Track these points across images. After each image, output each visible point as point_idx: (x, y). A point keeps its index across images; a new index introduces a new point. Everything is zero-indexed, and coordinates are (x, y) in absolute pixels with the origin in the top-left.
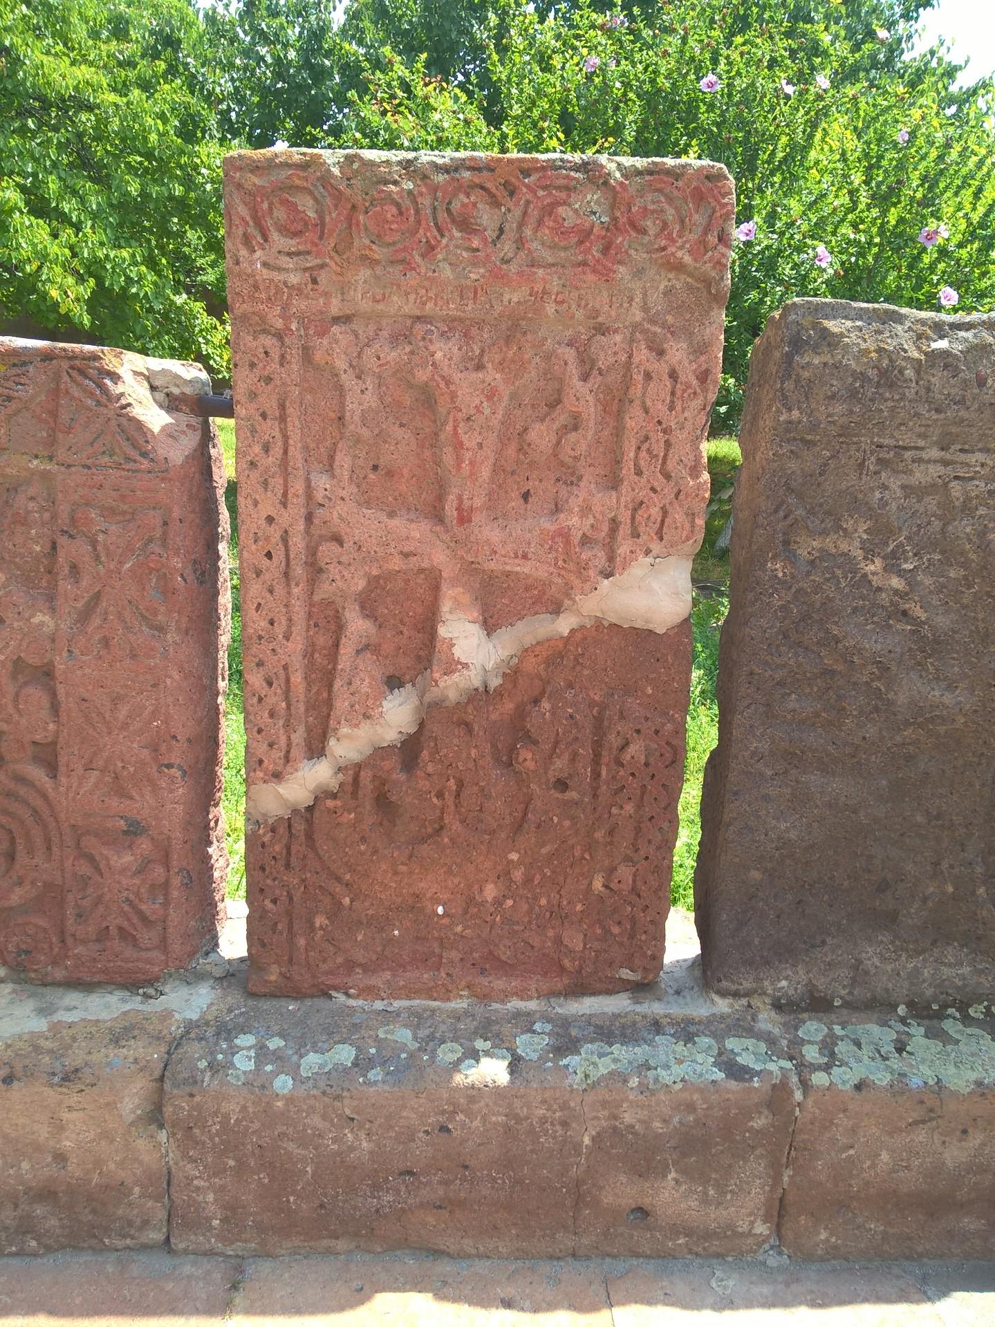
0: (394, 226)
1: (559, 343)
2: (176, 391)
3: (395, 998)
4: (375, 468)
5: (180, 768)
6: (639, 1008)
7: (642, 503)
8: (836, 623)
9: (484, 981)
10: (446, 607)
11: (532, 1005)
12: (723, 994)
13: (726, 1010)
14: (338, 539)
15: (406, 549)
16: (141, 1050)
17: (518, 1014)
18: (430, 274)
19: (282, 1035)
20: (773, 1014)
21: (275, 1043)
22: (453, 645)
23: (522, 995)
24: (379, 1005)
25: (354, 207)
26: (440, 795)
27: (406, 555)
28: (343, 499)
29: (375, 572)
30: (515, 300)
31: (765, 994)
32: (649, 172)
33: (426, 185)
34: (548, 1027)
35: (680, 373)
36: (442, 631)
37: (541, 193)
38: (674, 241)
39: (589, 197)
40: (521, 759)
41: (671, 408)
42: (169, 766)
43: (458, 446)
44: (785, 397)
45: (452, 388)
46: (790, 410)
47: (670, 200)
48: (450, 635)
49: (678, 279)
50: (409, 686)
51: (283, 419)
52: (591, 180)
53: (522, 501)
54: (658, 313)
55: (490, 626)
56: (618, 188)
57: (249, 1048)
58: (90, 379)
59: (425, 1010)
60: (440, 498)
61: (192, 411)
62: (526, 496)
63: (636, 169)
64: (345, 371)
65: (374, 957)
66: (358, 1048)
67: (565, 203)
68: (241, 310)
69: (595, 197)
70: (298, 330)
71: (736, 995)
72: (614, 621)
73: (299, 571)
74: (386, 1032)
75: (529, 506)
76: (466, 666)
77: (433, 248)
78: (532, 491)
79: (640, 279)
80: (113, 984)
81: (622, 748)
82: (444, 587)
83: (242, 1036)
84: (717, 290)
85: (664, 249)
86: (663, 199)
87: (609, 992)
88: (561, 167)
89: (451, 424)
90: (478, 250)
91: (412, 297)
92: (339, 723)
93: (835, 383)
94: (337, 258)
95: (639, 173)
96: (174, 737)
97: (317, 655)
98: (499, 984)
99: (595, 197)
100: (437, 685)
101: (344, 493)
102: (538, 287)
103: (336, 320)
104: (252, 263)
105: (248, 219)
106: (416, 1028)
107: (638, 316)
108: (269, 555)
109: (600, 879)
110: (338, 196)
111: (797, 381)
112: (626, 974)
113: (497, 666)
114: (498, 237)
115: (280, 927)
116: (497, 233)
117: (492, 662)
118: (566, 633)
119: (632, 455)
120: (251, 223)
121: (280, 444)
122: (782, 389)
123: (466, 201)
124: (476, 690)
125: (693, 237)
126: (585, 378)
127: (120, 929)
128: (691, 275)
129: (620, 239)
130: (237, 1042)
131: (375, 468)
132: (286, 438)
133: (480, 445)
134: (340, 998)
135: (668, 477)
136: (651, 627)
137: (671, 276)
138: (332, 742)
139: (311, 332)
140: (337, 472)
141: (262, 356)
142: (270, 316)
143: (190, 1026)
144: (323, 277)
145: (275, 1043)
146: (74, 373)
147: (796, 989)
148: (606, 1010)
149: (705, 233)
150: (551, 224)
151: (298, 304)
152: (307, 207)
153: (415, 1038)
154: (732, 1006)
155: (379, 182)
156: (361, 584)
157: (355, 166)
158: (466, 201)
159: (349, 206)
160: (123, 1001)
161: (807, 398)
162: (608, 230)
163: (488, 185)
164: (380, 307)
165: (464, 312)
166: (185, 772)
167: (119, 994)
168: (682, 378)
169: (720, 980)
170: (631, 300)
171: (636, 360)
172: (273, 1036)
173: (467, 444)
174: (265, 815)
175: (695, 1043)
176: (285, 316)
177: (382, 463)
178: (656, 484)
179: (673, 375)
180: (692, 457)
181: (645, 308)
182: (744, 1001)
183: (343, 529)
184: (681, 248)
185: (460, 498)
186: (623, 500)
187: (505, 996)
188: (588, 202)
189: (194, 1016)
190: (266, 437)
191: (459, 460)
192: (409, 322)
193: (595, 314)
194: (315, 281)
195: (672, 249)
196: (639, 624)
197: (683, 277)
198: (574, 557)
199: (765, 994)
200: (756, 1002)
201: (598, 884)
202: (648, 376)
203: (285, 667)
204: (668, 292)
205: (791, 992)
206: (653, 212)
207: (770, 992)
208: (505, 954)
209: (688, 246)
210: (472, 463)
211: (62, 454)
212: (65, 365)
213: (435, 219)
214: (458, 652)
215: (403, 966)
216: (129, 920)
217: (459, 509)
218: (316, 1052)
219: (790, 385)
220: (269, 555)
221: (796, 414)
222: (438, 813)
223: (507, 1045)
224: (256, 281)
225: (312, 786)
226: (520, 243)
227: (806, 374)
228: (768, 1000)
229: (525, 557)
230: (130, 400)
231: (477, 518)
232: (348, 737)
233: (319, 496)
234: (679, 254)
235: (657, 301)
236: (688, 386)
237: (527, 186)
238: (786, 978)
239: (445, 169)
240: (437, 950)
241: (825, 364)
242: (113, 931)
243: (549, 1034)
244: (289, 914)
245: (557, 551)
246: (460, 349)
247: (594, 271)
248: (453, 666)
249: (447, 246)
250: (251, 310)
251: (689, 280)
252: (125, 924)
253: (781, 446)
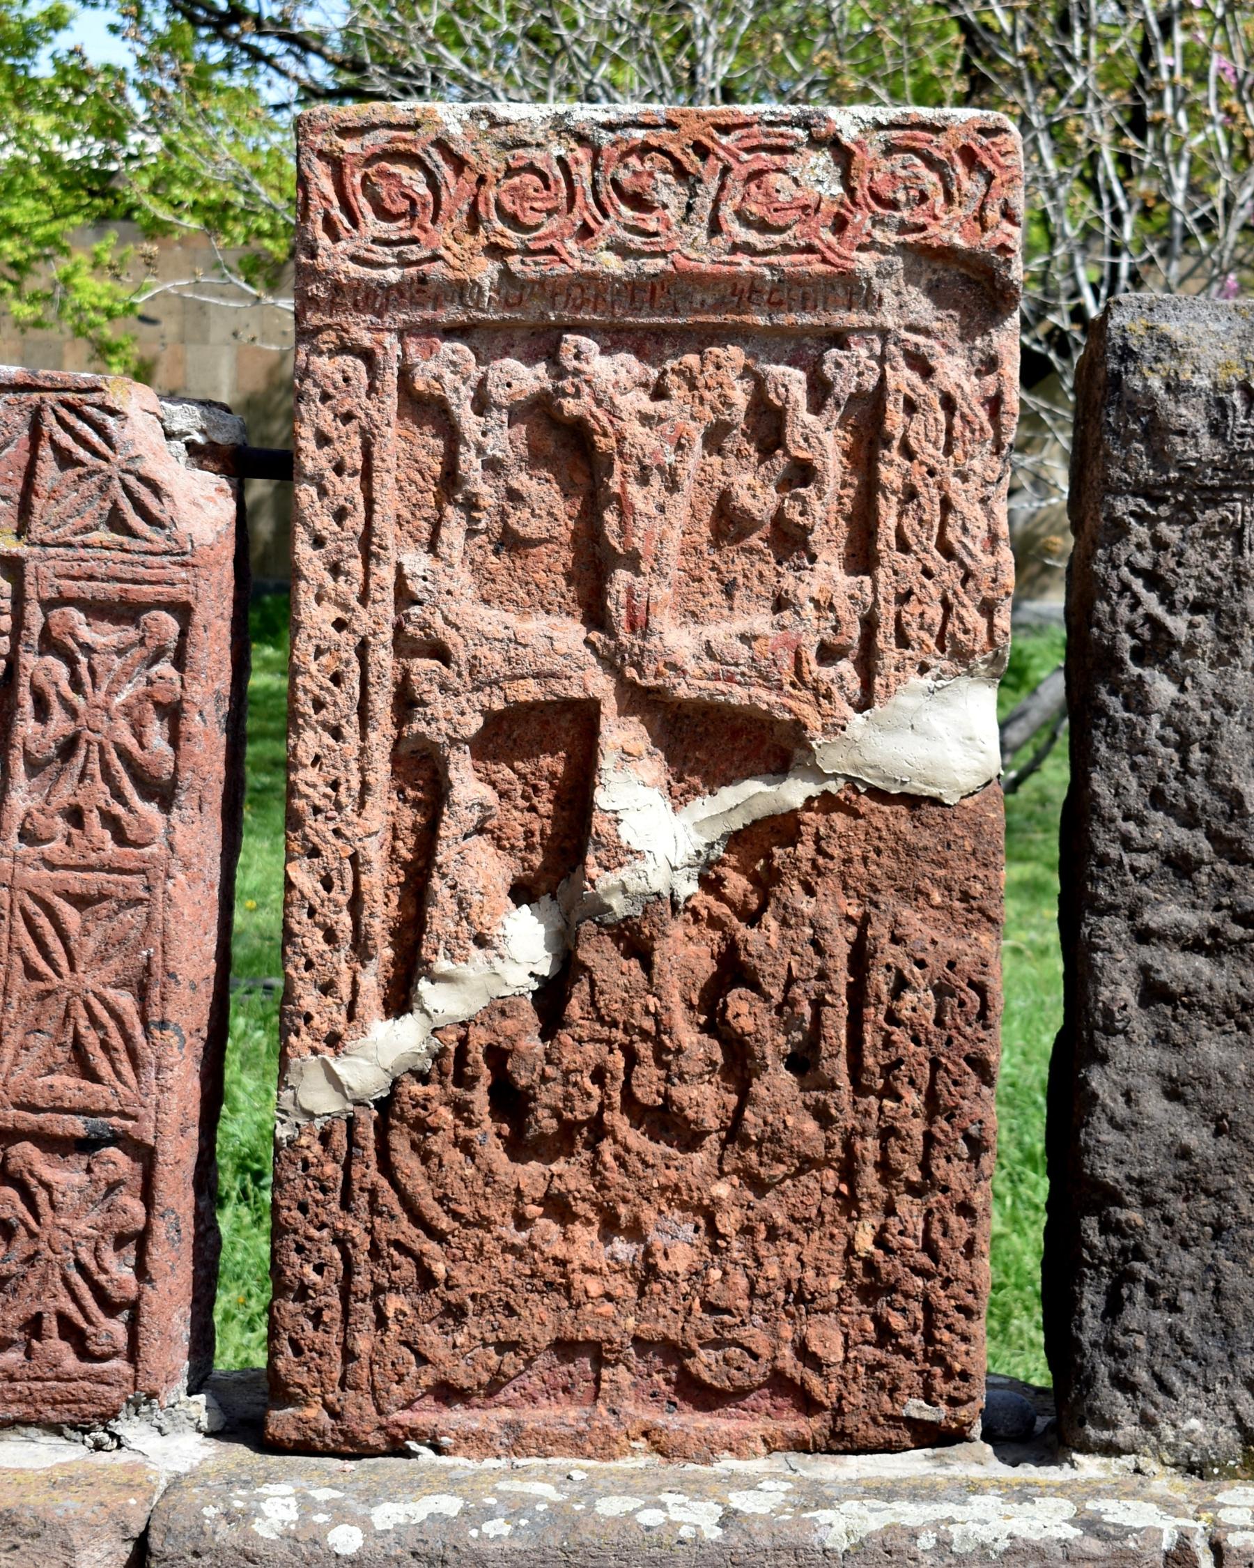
0: (537, 205)
2: (199, 439)
7: (910, 592)
10: (607, 762)
14: (441, 653)
25: (482, 180)
26: (599, 1075)
28: (449, 592)
29: (498, 705)
35: (959, 401)
37: (745, 156)
40: (730, 1015)
41: (948, 451)
47: (931, 162)
50: (545, 899)
51: (367, 474)
56: (854, 147)
65: (485, 1378)
67: (779, 170)
73: (382, 703)
81: (896, 994)
85: (923, 228)
86: (918, 161)
90: (656, 234)
92: (436, 952)
94: (456, 248)
101: (453, 586)
110: (459, 164)
115: (327, 1315)
117: (681, 853)
119: (892, 521)
120: (336, 203)
121: (361, 508)
124: (658, 894)
126: (816, 407)
132: (370, 503)
135: (947, 551)
140: (443, 549)
141: (341, 383)
146: (63, 412)
150: (761, 198)
155: (516, 146)
156: (474, 723)
158: (639, 168)
159: (475, 178)
162: (842, 204)
163: (673, 148)
171: (891, 384)
178: (930, 564)
179: (948, 403)
180: (984, 526)
182: (1128, 1461)
183: (451, 638)
185: (630, 592)
186: (881, 589)
190: (342, 502)
195: (931, 231)
198: (808, 678)
201: (865, 1242)
202: (910, 407)
203: (354, 858)
211: (38, 529)
212: (50, 398)
213: (596, 194)
214: (628, 834)
216: (76, 1299)
222: (594, 1107)
225: (389, 1060)
226: (715, 228)
230: (141, 450)
232: (447, 978)
233: (415, 586)
234: (945, 235)
244: (346, 1292)
247: (825, 260)
252: (71, 1308)
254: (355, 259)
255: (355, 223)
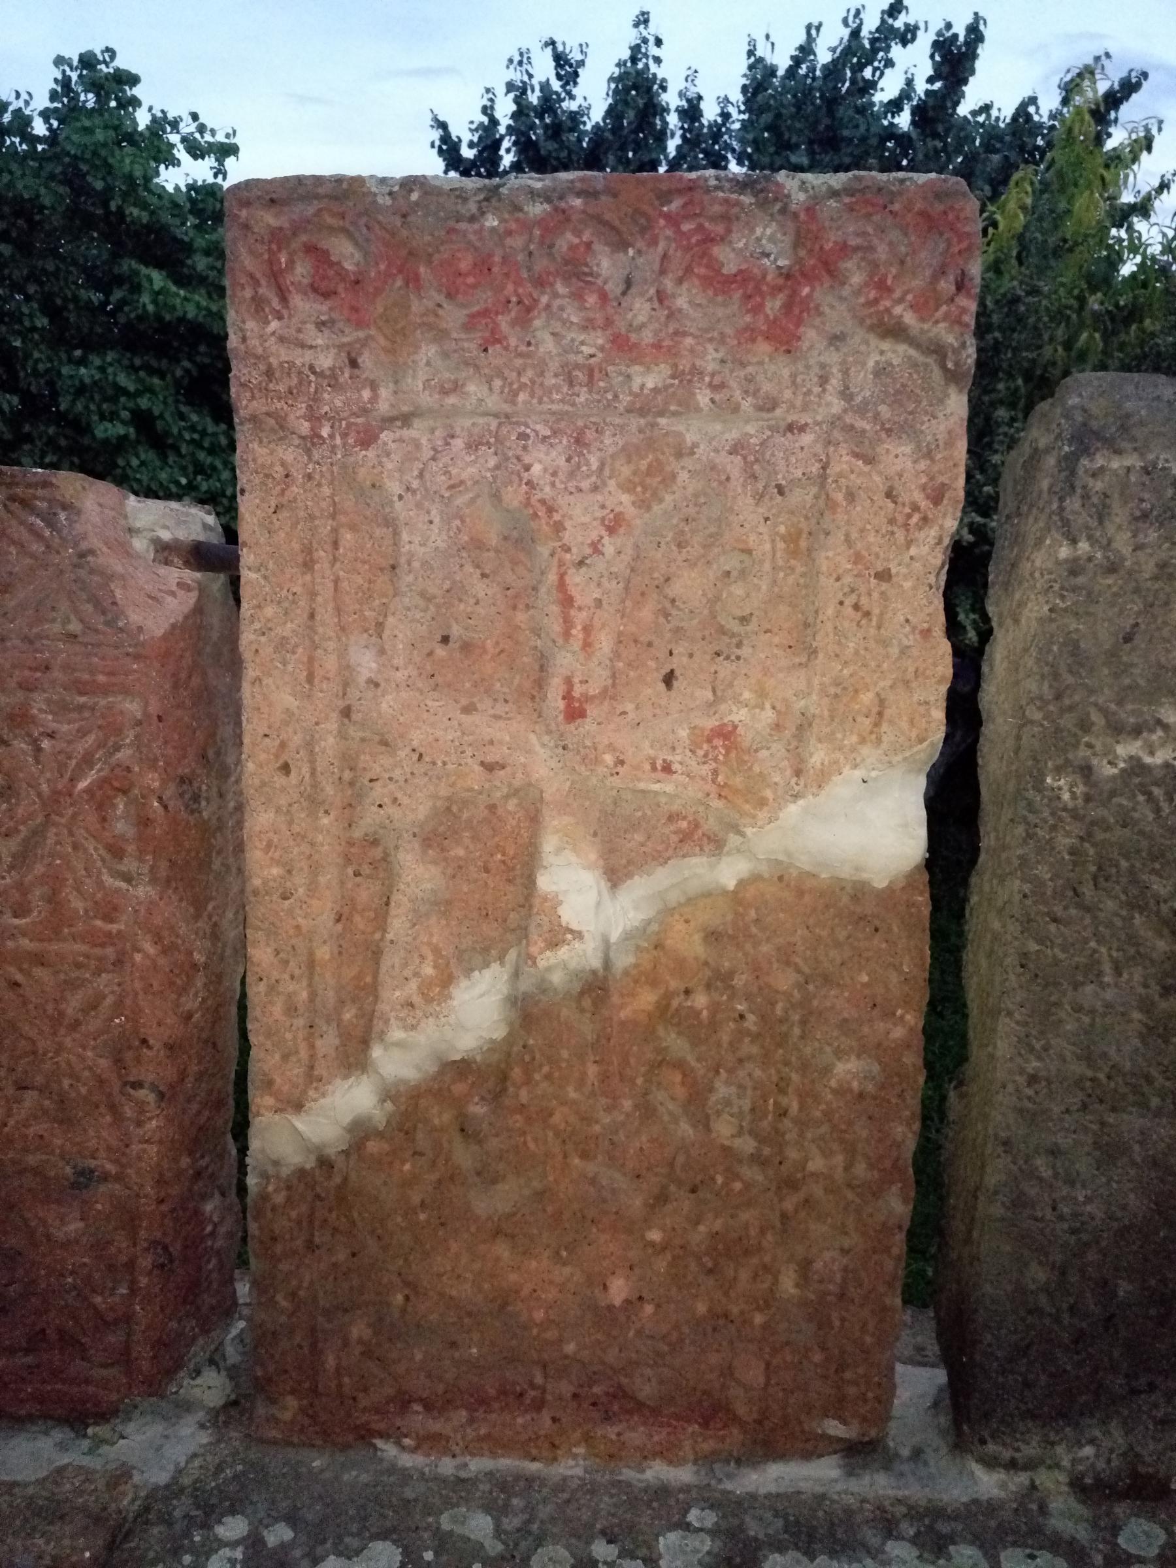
1: (716, 451)
2: (166, 536)
3: (472, 1455)
4: (445, 640)
5: (154, 1087)
6: (854, 1485)
8: (1153, 871)
9: (611, 1432)
10: (549, 843)
11: (684, 1475)
12: (991, 1463)
13: (996, 1492)
15: (489, 759)
16: (66, 1542)
17: (662, 1492)
18: (523, 348)
19: (292, 1519)
20: (1073, 1502)
21: (278, 1535)
22: (561, 903)
23: (669, 1453)
24: (447, 1466)
27: (489, 767)
30: (650, 384)
31: (1057, 1466)
32: (849, 191)
33: (517, 220)
34: (710, 1519)
36: (544, 882)
38: (890, 290)
39: (759, 231)
42: (137, 1085)
43: (567, 601)
44: (1066, 523)
45: (556, 517)
46: (1074, 541)
48: (554, 888)
49: (895, 352)
52: (763, 204)
53: (662, 686)
54: (866, 402)
55: (615, 876)
57: (233, 1545)
58: (38, 515)
59: (518, 1478)
60: (540, 684)
61: (187, 564)
62: (669, 679)
63: (830, 187)
64: (400, 497)
66: (406, 1552)
68: (250, 411)
69: (768, 231)
70: (332, 436)
71: (1012, 1465)
72: (807, 868)
74: (454, 1520)
75: (673, 693)
76: (579, 935)
77: (529, 310)
78: (677, 673)
79: (837, 349)
80: (51, 1417)
82: (547, 813)
83: (229, 1520)
84: (957, 364)
87: (808, 1455)
88: (716, 188)
89: (554, 570)
91: (498, 383)
93: (1146, 496)
95: (834, 194)
96: (144, 1041)
97: (357, 918)
98: (637, 1436)
99: (768, 231)
100: (534, 963)
102: (684, 364)
103: (389, 421)
104: (263, 338)
105: (258, 275)
106: (497, 1510)
107: (836, 405)
108: (286, 768)
109: (792, 1274)
111: (1086, 497)
112: (834, 1428)
113: (628, 936)
114: (624, 293)
116: (622, 287)
117: (620, 929)
118: (731, 885)
122: (1062, 509)
123: (576, 241)
125: (917, 283)
127: (61, 1332)
128: (912, 342)
129: (806, 290)
130: (220, 1531)
131: (445, 640)
133: (599, 603)
134: (389, 1450)
136: (865, 876)
137: (886, 345)
138: (377, 1052)
139: (351, 441)
142: (292, 417)
143: (155, 1494)
144: (366, 360)
145: (278, 1535)
146: (15, 506)
147: (1109, 1461)
148: (803, 1486)
149: (935, 278)
151: (333, 401)
152: (346, 253)
153: (498, 1532)
154: (1003, 1486)
157: (415, 196)
160: (62, 1447)
161: (1101, 523)
164: (452, 400)
165: (573, 405)
166: (161, 1096)
167: (58, 1435)
168: (905, 497)
169: (983, 1442)
170: (823, 380)
171: (834, 469)
172: (276, 1520)
173: (579, 600)
174: (276, 1163)
175: (949, 1558)
176: (314, 418)
177: (456, 631)
181: (846, 394)
182: (1023, 1478)
184: (901, 300)
185: (569, 682)
187: (647, 1455)
188: (759, 240)
189: (161, 1477)
191: (568, 623)
192: (494, 424)
193: (769, 405)
194: (354, 363)
196: (846, 873)
197: (902, 348)
199: (1057, 1466)
200: (1046, 1479)
201: (788, 1284)
204: (880, 372)
205: (1101, 1465)
206: (857, 249)
207: (1066, 1463)
208: (646, 1390)
209: (910, 297)
210: (587, 629)
214: (568, 915)
215: (484, 1402)
217: (568, 697)
218: (339, 1554)
219: (1073, 504)
220: (286, 768)
221: (1084, 546)
223: (643, 1552)
224: (270, 365)
225: (347, 1120)
227: (1098, 485)
228: (1063, 1478)
229: (667, 769)
231: (592, 711)
232: (399, 1044)
234: (898, 310)
235: (863, 383)
236: (915, 508)
237: (667, 217)
238: (1092, 1441)
239: (545, 196)
240: (539, 1380)
241: (1129, 469)
242: (52, 1334)
243: (709, 1532)
245: (715, 759)
246: (568, 460)
248: (558, 936)
249: (548, 306)
250: (264, 409)
251: (912, 352)
253: (1063, 597)
254: (282, 340)
255: (284, 299)
